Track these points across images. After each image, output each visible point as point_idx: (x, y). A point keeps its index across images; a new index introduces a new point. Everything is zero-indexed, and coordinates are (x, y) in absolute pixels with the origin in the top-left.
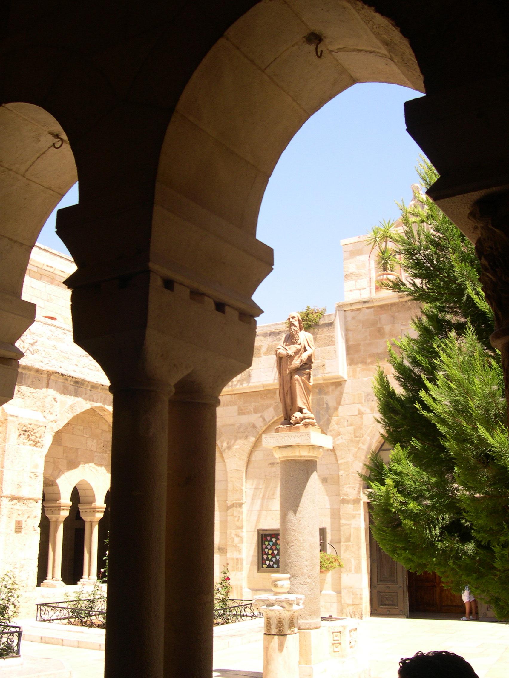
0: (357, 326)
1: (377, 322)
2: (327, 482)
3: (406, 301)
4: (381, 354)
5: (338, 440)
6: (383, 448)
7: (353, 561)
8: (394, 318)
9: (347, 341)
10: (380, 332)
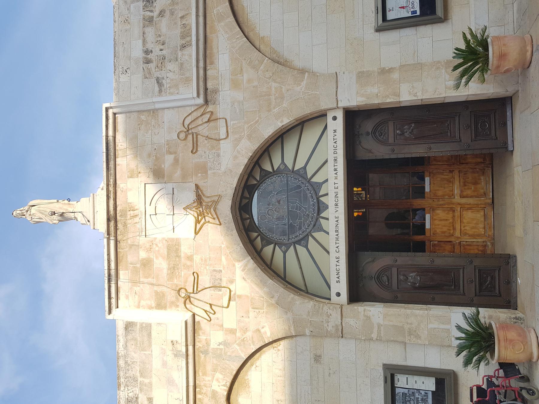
0: (136, 293)
1: (134, 267)
2: (320, 356)
4: (169, 265)
5: (266, 333)
7: (431, 326)
8: (133, 245)
9: (150, 308)
10: (147, 264)
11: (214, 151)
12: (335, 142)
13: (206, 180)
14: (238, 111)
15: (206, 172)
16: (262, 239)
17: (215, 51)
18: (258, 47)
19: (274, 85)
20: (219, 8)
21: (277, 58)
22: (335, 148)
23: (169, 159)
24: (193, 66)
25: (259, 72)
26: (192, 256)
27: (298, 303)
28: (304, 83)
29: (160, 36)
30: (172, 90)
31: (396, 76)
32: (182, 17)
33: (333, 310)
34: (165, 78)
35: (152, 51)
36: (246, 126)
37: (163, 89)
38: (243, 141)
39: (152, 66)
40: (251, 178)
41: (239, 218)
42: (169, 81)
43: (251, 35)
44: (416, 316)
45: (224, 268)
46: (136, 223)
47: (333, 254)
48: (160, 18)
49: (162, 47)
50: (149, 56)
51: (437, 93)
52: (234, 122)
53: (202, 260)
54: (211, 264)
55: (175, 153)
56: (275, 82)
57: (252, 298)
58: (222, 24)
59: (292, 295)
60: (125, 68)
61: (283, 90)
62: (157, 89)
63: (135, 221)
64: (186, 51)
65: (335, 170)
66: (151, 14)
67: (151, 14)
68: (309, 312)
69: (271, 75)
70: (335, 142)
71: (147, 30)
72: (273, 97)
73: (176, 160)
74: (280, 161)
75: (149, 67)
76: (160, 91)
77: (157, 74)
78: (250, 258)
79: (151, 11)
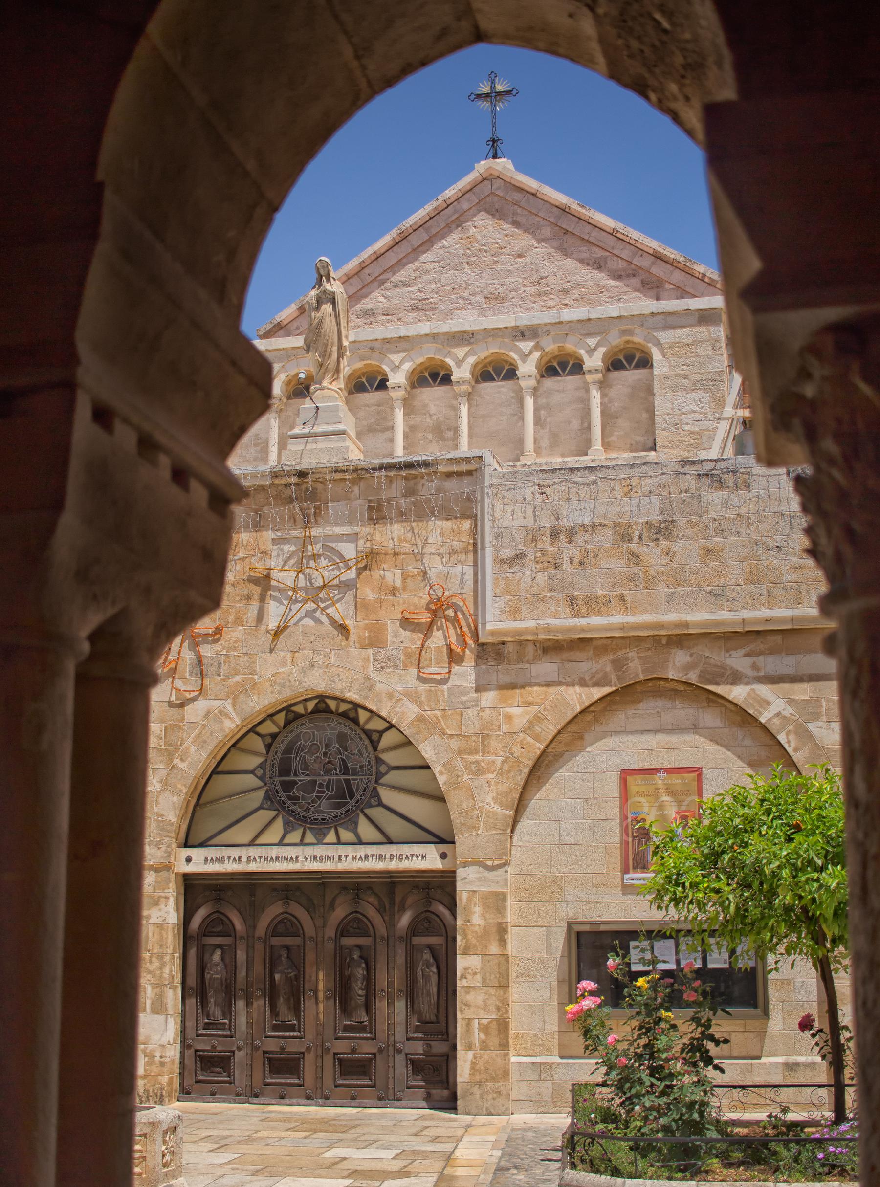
3: (286, 485)
6: (220, 769)
11: (403, 657)
12: (407, 857)
13: (357, 646)
14: (464, 698)
15: (371, 645)
16: (274, 736)
17: (565, 655)
18: (568, 729)
19: (499, 760)
20: (637, 662)
21: (546, 762)
22: (400, 858)
23: (393, 577)
24: (538, 621)
25: (521, 734)
26: (242, 625)
27: (175, 799)
28: (497, 808)
29: (596, 556)
30: (501, 582)
31: (494, 949)
32: (622, 598)
33: (165, 852)
34: (524, 569)
35: (571, 542)
36: (439, 713)
37: (505, 566)
38: (415, 709)
39: (546, 544)
40: (368, 714)
41: (305, 697)
42: (517, 578)
43: (590, 717)
44: (161, 969)
45: (224, 680)
46: (295, 521)
47: (244, 852)
48: (626, 557)
49: (576, 560)
50: (562, 537)
51: (464, 1007)
52: (446, 693)
53: (237, 641)
54: (228, 658)
55: (404, 588)
56: (503, 762)
57: (180, 727)
58: (609, 668)
59: (185, 790)
60: (548, 491)
61: (490, 775)
62: (506, 554)
63: (297, 518)
64: (564, 609)
65: (366, 857)
66: (636, 537)
67: (636, 537)
68: (162, 816)
69: (515, 755)
70: (407, 857)
71: (609, 532)
72: (479, 757)
73: (393, 591)
74: (393, 763)
75: (544, 538)
76: (502, 561)
77: (531, 554)
78: (238, 722)
79: (640, 538)
